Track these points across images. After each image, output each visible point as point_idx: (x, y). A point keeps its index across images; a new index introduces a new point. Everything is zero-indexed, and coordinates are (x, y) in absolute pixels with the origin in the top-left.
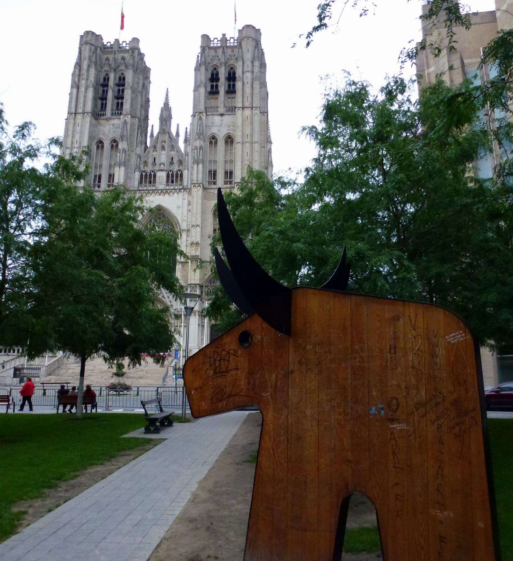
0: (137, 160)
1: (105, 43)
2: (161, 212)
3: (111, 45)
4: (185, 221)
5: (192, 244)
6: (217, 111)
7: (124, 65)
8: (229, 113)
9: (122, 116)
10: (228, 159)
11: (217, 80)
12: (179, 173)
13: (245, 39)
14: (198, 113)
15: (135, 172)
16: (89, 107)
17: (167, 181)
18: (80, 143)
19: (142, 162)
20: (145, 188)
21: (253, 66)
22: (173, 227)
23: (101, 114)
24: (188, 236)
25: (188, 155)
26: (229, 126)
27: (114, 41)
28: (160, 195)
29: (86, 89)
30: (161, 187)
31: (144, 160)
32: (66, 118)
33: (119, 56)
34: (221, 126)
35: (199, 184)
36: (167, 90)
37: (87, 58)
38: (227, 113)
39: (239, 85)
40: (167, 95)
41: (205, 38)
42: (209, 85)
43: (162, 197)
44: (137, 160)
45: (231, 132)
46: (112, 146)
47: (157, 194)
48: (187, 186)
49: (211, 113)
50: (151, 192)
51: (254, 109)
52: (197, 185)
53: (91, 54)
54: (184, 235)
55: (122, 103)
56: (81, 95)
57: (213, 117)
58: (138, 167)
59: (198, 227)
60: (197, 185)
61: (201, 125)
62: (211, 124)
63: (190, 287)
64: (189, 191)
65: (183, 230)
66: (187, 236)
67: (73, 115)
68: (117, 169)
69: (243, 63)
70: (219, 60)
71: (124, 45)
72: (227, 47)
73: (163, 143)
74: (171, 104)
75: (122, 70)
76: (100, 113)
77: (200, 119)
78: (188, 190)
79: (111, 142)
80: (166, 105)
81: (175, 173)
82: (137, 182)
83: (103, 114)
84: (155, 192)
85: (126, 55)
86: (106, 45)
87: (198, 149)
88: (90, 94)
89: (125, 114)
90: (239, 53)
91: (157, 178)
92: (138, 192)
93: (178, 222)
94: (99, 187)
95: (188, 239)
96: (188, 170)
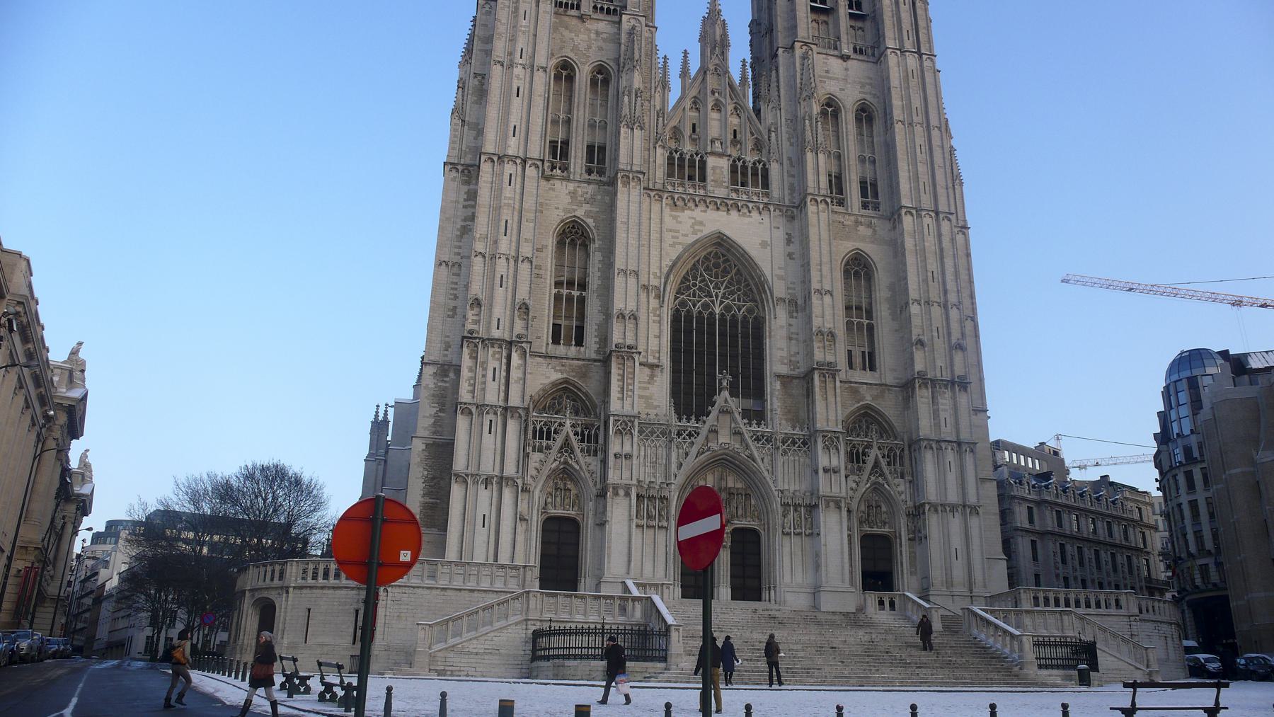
0: (658, 120)
4: (780, 278)
8: (861, 57)
10: (867, 155)
12: (760, 167)
17: (734, 181)
25: (776, 129)
26: (863, 86)
28: (718, 209)
30: (722, 192)
34: (844, 80)
35: (823, 196)
38: (857, 57)
43: (723, 214)
44: (658, 120)
45: (868, 97)
46: (594, 82)
47: (711, 207)
51: (924, 57)
57: (826, 59)
64: (787, 210)
73: (716, 94)
74: (724, 16)
82: (662, 170)
92: (666, 195)
93: (767, 282)
94: (565, 168)
95: (793, 321)
96: (782, 164)
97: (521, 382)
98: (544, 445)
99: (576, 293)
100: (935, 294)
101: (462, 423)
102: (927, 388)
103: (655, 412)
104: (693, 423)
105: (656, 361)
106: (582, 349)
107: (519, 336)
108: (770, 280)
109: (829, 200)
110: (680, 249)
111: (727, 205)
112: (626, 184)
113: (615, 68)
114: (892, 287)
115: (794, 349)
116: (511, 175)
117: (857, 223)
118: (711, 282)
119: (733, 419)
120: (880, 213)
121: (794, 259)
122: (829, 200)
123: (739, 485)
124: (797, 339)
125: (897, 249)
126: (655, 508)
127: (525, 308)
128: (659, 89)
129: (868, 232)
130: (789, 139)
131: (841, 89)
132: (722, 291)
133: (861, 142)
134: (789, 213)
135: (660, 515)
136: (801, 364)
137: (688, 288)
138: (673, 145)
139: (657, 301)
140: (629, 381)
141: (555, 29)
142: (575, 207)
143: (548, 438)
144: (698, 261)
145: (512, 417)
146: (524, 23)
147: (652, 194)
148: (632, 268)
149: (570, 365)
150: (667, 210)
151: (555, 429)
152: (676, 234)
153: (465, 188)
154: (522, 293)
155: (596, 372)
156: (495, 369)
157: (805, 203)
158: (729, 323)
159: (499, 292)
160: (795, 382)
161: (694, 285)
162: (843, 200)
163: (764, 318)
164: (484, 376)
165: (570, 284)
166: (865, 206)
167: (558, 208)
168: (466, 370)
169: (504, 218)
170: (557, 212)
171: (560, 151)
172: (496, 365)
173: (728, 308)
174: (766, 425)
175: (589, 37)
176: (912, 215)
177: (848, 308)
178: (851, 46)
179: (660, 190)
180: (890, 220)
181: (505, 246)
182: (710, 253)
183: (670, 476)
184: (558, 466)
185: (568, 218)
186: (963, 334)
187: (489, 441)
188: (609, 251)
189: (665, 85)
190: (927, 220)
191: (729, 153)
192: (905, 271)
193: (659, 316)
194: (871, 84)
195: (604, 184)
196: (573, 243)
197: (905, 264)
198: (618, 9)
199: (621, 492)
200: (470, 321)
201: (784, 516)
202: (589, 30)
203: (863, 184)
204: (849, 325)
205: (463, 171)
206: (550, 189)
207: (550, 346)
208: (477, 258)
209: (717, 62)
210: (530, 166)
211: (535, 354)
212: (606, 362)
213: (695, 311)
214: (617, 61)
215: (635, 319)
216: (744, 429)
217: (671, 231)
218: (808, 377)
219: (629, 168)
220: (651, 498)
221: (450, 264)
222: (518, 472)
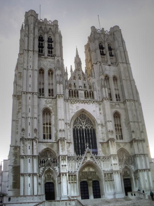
0: (66, 82)
2: (83, 113)
3: (42, 21)
4: (99, 119)
6: (107, 63)
8: (113, 65)
9: (56, 57)
10: (116, 88)
12: (91, 92)
13: (117, 32)
14: (99, 62)
15: (66, 89)
16: (37, 49)
17: (85, 96)
18: (33, 68)
19: (68, 84)
21: (123, 45)
22: (92, 122)
23: (41, 55)
25: (95, 83)
26: (114, 72)
27: (44, 19)
28: (82, 103)
31: (69, 83)
32: (19, 53)
33: (48, 27)
36: (77, 48)
40: (77, 51)
41: (93, 28)
43: (83, 104)
44: (66, 82)
46: (49, 74)
47: (81, 103)
51: (128, 64)
52: (106, 99)
55: (52, 52)
60: (106, 99)
61: (102, 68)
62: (105, 69)
64: (99, 103)
65: (99, 124)
75: (50, 34)
76: (40, 54)
78: (98, 102)
79: (48, 71)
81: (89, 92)
84: (80, 101)
85: (52, 28)
87: (104, 80)
91: (79, 94)
94: (43, 95)
95: (103, 129)
96: (97, 91)
97: (36, 149)
98: (43, 164)
99: (48, 126)
101: (22, 161)
103: (71, 154)
104: (80, 156)
105: (70, 142)
106: (51, 140)
107: (35, 137)
109: (109, 99)
111: (84, 102)
112: (59, 98)
113: (54, 70)
114: (125, 119)
115: (103, 136)
116: (30, 97)
117: (116, 104)
121: (101, 114)
122: (109, 99)
124: (104, 134)
125: (126, 110)
127: (36, 130)
130: (98, 85)
131: (109, 73)
132: (85, 123)
133: (115, 85)
134: (99, 103)
136: (105, 139)
137: (76, 123)
138: (70, 88)
139: (69, 127)
140: (64, 147)
141: (39, 61)
142: (47, 105)
143: (44, 163)
144: (78, 116)
145: (35, 158)
147: (66, 100)
149: (49, 144)
150: (70, 104)
151: (46, 160)
152: (72, 110)
153: (18, 101)
154: (35, 126)
155: (55, 145)
156: (29, 146)
157: (103, 100)
158: (87, 131)
159: (29, 127)
160: (105, 144)
161: (78, 122)
162: (112, 99)
163: (95, 129)
164: (27, 148)
166: (117, 100)
167: (42, 105)
168: (22, 147)
170: (42, 106)
171: (41, 91)
172: (29, 145)
173: (86, 127)
176: (128, 101)
177: (115, 125)
178: (111, 63)
179: (68, 99)
180: (123, 103)
181: (30, 115)
182: (81, 114)
183: (76, 169)
184: (47, 170)
185: (45, 107)
187: (29, 165)
188: (56, 115)
191: (83, 89)
192: (128, 115)
193: (70, 130)
195: (54, 99)
196: (47, 114)
197: (128, 113)
198: (54, 55)
199: (64, 175)
200: (22, 134)
202: (47, 61)
203: (116, 95)
204: (116, 129)
205: (17, 97)
206: (40, 100)
208: (23, 118)
210: (35, 95)
211: (39, 142)
212: (58, 143)
213: (78, 129)
214: (55, 68)
215: (64, 131)
218: (108, 142)
219: (60, 94)
220: (72, 176)
221: (16, 121)
222: (37, 172)
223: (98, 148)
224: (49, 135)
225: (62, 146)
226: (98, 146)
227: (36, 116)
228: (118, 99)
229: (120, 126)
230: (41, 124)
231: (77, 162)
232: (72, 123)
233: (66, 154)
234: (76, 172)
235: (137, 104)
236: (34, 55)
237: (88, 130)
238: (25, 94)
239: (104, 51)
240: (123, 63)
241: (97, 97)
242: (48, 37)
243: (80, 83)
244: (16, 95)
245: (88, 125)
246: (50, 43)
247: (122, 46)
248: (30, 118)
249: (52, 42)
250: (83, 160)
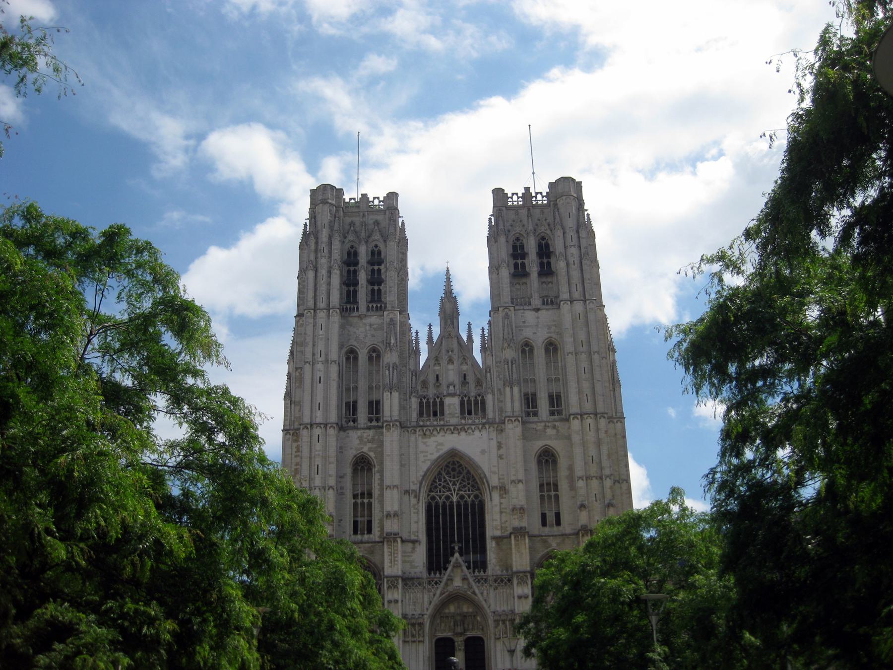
1: (347, 200)
4: (494, 473)
5: (513, 509)
6: (530, 304)
7: (378, 234)
9: (386, 313)
10: (553, 377)
11: (524, 256)
12: (479, 399)
13: (564, 198)
15: (410, 398)
17: (462, 412)
18: (326, 355)
19: (420, 381)
20: (428, 423)
21: (579, 238)
22: (477, 483)
23: (350, 308)
24: (501, 497)
26: (549, 328)
27: (360, 196)
28: (452, 433)
29: (329, 272)
30: (454, 421)
31: (422, 379)
34: (537, 326)
37: (327, 225)
39: (560, 266)
41: (499, 194)
42: (512, 262)
45: (554, 336)
46: (370, 358)
47: (448, 432)
48: (495, 419)
49: (522, 307)
50: (438, 429)
51: (587, 302)
52: (513, 419)
53: (332, 219)
54: (496, 496)
55: (379, 291)
56: (322, 283)
58: (413, 391)
59: (520, 483)
60: (513, 419)
62: (521, 324)
63: (517, 576)
66: (500, 495)
67: (312, 311)
68: (387, 395)
69: (564, 233)
70: (523, 226)
71: (376, 202)
72: (533, 206)
77: (507, 316)
78: (496, 426)
79: (369, 352)
80: (448, 294)
81: (473, 399)
83: (354, 308)
85: (380, 218)
86: (348, 203)
87: (510, 364)
88: (336, 280)
89: (390, 309)
90: (554, 219)
91: (446, 408)
93: (485, 475)
94: (354, 421)
95: (503, 501)
96: (493, 395)
100: (593, 470)
102: (587, 535)
104: (438, 574)
105: (415, 538)
106: (371, 536)
108: (487, 475)
110: (429, 463)
112: (388, 430)
115: (504, 519)
117: (546, 427)
118: (451, 481)
119: (462, 570)
120: (563, 416)
122: (520, 419)
123: (471, 610)
124: (506, 512)
126: (415, 630)
128: (413, 356)
129: (554, 432)
134: (499, 428)
135: (419, 634)
137: (436, 487)
141: (342, 327)
146: (321, 332)
147: (410, 430)
148: (395, 484)
153: (295, 445)
158: (463, 507)
160: (506, 540)
161: (440, 485)
165: (363, 494)
166: (552, 413)
167: (351, 448)
169: (317, 463)
173: (462, 497)
174: (485, 572)
175: (366, 330)
176: (578, 419)
177: (541, 486)
181: (318, 482)
182: (449, 463)
186: (613, 496)
189: (417, 352)
190: (589, 421)
191: (458, 393)
194: (555, 325)
196: (363, 469)
201: (496, 627)
202: (365, 324)
205: (293, 434)
207: (353, 536)
209: (450, 329)
213: (441, 502)
216: (469, 576)
217: (422, 452)
223: (488, 552)
224: (368, 521)
225: (391, 553)
226: (488, 547)
227: (332, 482)
228: (556, 408)
229: (556, 486)
230: (348, 497)
231: (429, 592)
232: (424, 490)
233: (400, 573)
234: (423, 615)
235: (603, 422)
236: (328, 316)
237: (466, 502)
238: (307, 428)
239: (526, 261)
240: (571, 301)
241: (494, 412)
242: (370, 250)
243: (451, 374)
244: (290, 430)
245: (465, 491)
246: (376, 268)
247: (574, 246)
248: (317, 488)
249: (380, 264)
250: (442, 584)
